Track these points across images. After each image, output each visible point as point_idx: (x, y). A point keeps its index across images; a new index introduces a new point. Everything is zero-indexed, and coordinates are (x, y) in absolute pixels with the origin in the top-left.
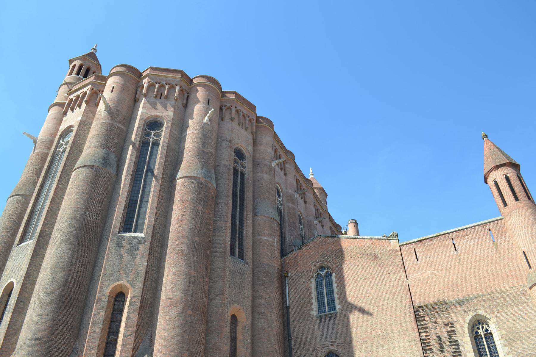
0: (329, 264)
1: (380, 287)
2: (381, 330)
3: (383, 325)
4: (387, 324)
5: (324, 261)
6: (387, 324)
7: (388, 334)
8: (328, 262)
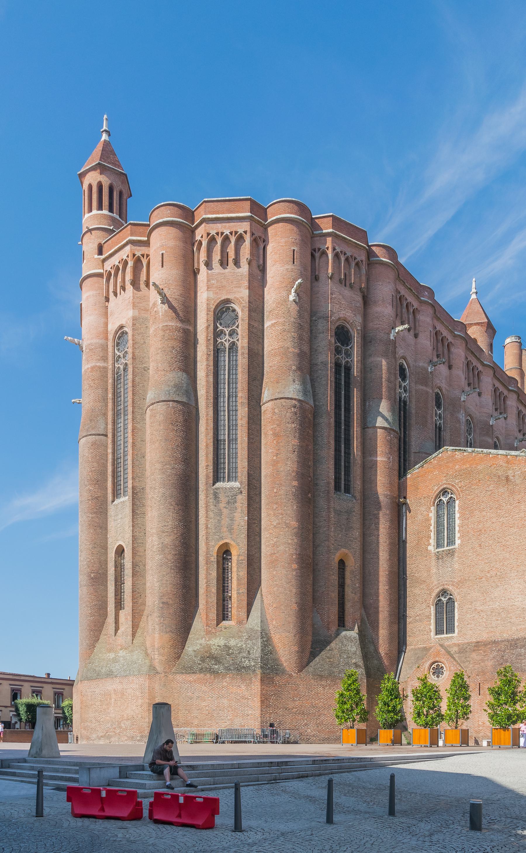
0: (453, 489)
3: (502, 564)
5: (449, 484)
6: (506, 563)
8: (453, 486)
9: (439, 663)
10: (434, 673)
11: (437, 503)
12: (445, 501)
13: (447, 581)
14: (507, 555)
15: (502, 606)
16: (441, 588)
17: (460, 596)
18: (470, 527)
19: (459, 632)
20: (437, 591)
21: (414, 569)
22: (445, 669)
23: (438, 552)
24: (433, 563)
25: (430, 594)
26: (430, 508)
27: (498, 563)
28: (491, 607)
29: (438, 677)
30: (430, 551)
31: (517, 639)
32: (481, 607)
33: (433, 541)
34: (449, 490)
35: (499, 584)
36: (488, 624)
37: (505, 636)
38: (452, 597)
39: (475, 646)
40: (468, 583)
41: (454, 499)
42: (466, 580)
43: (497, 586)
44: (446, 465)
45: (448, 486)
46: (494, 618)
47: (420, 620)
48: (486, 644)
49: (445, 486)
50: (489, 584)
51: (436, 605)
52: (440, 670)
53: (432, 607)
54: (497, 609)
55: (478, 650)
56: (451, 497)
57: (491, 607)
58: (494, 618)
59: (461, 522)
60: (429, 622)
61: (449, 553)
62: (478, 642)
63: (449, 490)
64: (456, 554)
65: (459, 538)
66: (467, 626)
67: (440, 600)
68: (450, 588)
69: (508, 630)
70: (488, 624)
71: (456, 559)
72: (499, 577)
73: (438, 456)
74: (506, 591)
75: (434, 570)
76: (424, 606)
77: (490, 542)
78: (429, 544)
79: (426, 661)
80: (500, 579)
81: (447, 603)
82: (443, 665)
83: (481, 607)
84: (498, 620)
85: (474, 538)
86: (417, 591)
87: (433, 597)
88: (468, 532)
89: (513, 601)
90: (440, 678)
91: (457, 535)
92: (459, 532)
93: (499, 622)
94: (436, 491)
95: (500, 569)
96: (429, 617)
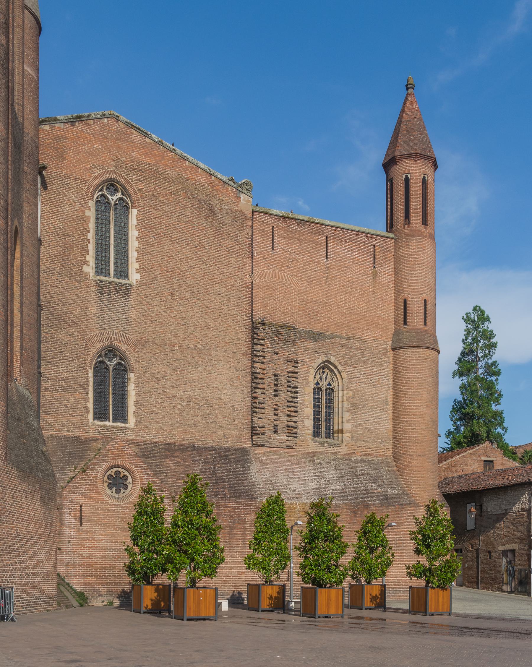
0: (128, 187)
1: (210, 268)
2: (200, 339)
3: (204, 333)
4: (210, 334)
5: (120, 175)
7: (208, 349)
8: (127, 181)
9: (120, 469)
10: (110, 486)
11: (97, 198)
12: (111, 200)
13: (116, 334)
14: (212, 323)
15: (204, 397)
16: (107, 343)
17: (139, 366)
18: (155, 259)
19: (138, 422)
20: (97, 346)
21: (57, 298)
22: (130, 480)
23: (101, 281)
24: (93, 297)
25: (87, 348)
26: (86, 202)
27: (198, 329)
28: (188, 393)
29: (118, 491)
30: (87, 274)
31: (225, 448)
32: (173, 391)
33: (91, 258)
34: (119, 186)
35: (200, 362)
36: (184, 419)
37: (209, 442)
38: (123, 362)
39: (166, 450)
40: (152, 347)
41: (127, 203)
42: (148, 341)
43: (197, 365)
44: (115, 143)
45: (120, 179)
46: (192, 412)
47: (68, 389)
48: (184, 449)
49: (114, 176)
50: (185, 358)
51: (94, 369)
52: (120, 481)
53: (90, 370)
54: (197, 399)
55: (173, 456)
56: (121, 199)
57: (188, 393)
58: (192, 412)
59: (141, 245)
60: (83, 396)
61: (121, 290)
62: (168, 444)
63: (119, 186)
64: (133, 296)
65: (138, 271)
66: (152, 415)
67: (102, 362)
68: (123, 347)
69: (212, 434)
70: (184, 419)
71: (132, 303)
72: (199, 352)
73: (102, 120)
74: (209, 375)
75: (94, 310)
76: (75, 365)
77: (186, 294)
78: (86, 263)
79: (99, 463)
80: (202, 356)
81: (113, 370)
82: (126, 473)
83: (173, 391)
84: (197, 416)
85: (162, 280)
86: (61, 336)
87: (91, 354)
88: (153, 266)
89: (219, 392)
90: (121, 495)
91: (133, 266)
92: (138, 260)
93: (200, 419)
94: (97, 177)
95: (201, 340)
96: (84, 386)
